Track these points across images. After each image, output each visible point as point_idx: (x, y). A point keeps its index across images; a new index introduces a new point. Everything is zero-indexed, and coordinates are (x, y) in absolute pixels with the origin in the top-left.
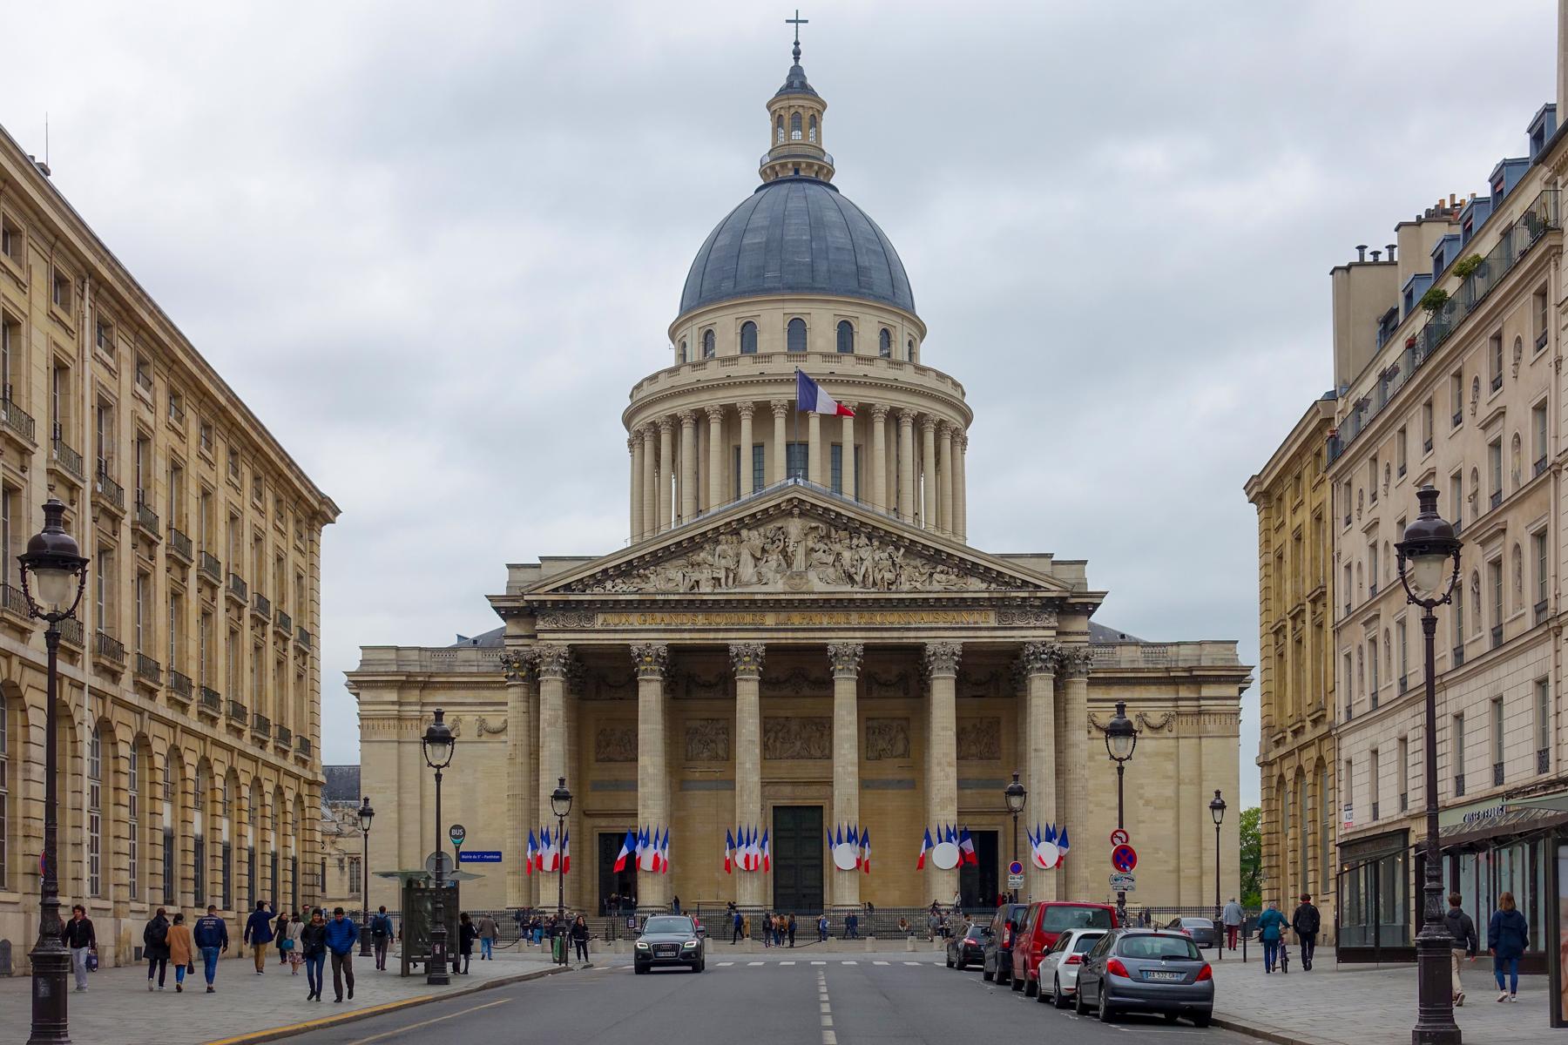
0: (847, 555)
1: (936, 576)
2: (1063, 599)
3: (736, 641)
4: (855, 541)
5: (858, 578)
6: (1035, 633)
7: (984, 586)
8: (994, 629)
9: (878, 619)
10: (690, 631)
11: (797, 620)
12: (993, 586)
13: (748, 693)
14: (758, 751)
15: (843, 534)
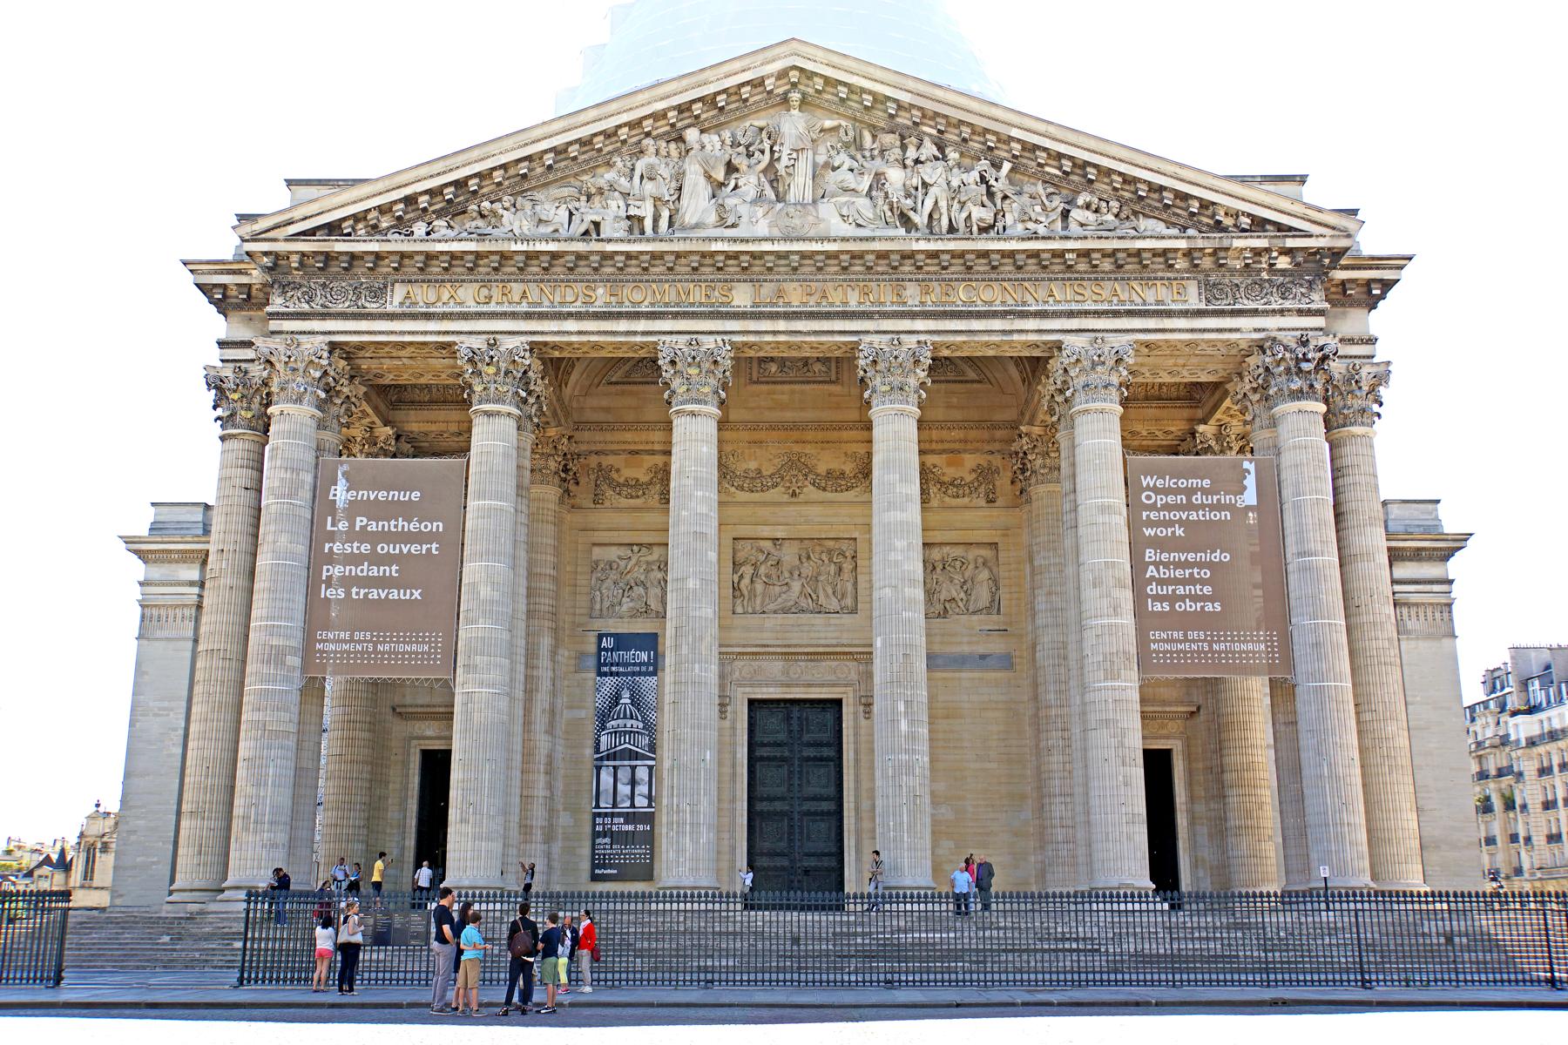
0: (895, 176)
1: (1077, 214)
2: (1337, 254)
3: (669, 337)
4: (912, 153)
5: (920, 219)
6: (1284, 323)
7: (1174, 232)
8: (1200, 313)
9: (961, 296)
10: (579, 316)
11: (795, 296)
12: (1191, 232)
13: (695, 439)
14: (713, 556)
15: (890, 139)
